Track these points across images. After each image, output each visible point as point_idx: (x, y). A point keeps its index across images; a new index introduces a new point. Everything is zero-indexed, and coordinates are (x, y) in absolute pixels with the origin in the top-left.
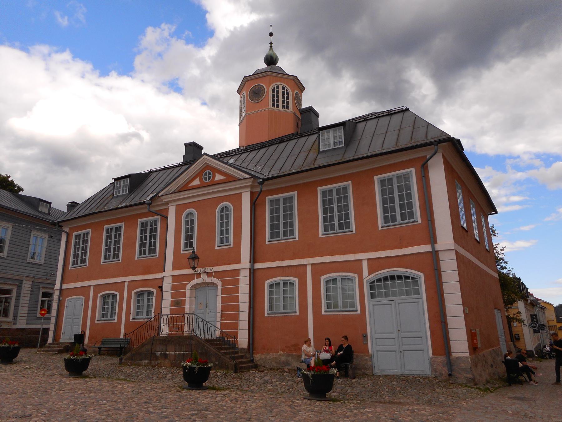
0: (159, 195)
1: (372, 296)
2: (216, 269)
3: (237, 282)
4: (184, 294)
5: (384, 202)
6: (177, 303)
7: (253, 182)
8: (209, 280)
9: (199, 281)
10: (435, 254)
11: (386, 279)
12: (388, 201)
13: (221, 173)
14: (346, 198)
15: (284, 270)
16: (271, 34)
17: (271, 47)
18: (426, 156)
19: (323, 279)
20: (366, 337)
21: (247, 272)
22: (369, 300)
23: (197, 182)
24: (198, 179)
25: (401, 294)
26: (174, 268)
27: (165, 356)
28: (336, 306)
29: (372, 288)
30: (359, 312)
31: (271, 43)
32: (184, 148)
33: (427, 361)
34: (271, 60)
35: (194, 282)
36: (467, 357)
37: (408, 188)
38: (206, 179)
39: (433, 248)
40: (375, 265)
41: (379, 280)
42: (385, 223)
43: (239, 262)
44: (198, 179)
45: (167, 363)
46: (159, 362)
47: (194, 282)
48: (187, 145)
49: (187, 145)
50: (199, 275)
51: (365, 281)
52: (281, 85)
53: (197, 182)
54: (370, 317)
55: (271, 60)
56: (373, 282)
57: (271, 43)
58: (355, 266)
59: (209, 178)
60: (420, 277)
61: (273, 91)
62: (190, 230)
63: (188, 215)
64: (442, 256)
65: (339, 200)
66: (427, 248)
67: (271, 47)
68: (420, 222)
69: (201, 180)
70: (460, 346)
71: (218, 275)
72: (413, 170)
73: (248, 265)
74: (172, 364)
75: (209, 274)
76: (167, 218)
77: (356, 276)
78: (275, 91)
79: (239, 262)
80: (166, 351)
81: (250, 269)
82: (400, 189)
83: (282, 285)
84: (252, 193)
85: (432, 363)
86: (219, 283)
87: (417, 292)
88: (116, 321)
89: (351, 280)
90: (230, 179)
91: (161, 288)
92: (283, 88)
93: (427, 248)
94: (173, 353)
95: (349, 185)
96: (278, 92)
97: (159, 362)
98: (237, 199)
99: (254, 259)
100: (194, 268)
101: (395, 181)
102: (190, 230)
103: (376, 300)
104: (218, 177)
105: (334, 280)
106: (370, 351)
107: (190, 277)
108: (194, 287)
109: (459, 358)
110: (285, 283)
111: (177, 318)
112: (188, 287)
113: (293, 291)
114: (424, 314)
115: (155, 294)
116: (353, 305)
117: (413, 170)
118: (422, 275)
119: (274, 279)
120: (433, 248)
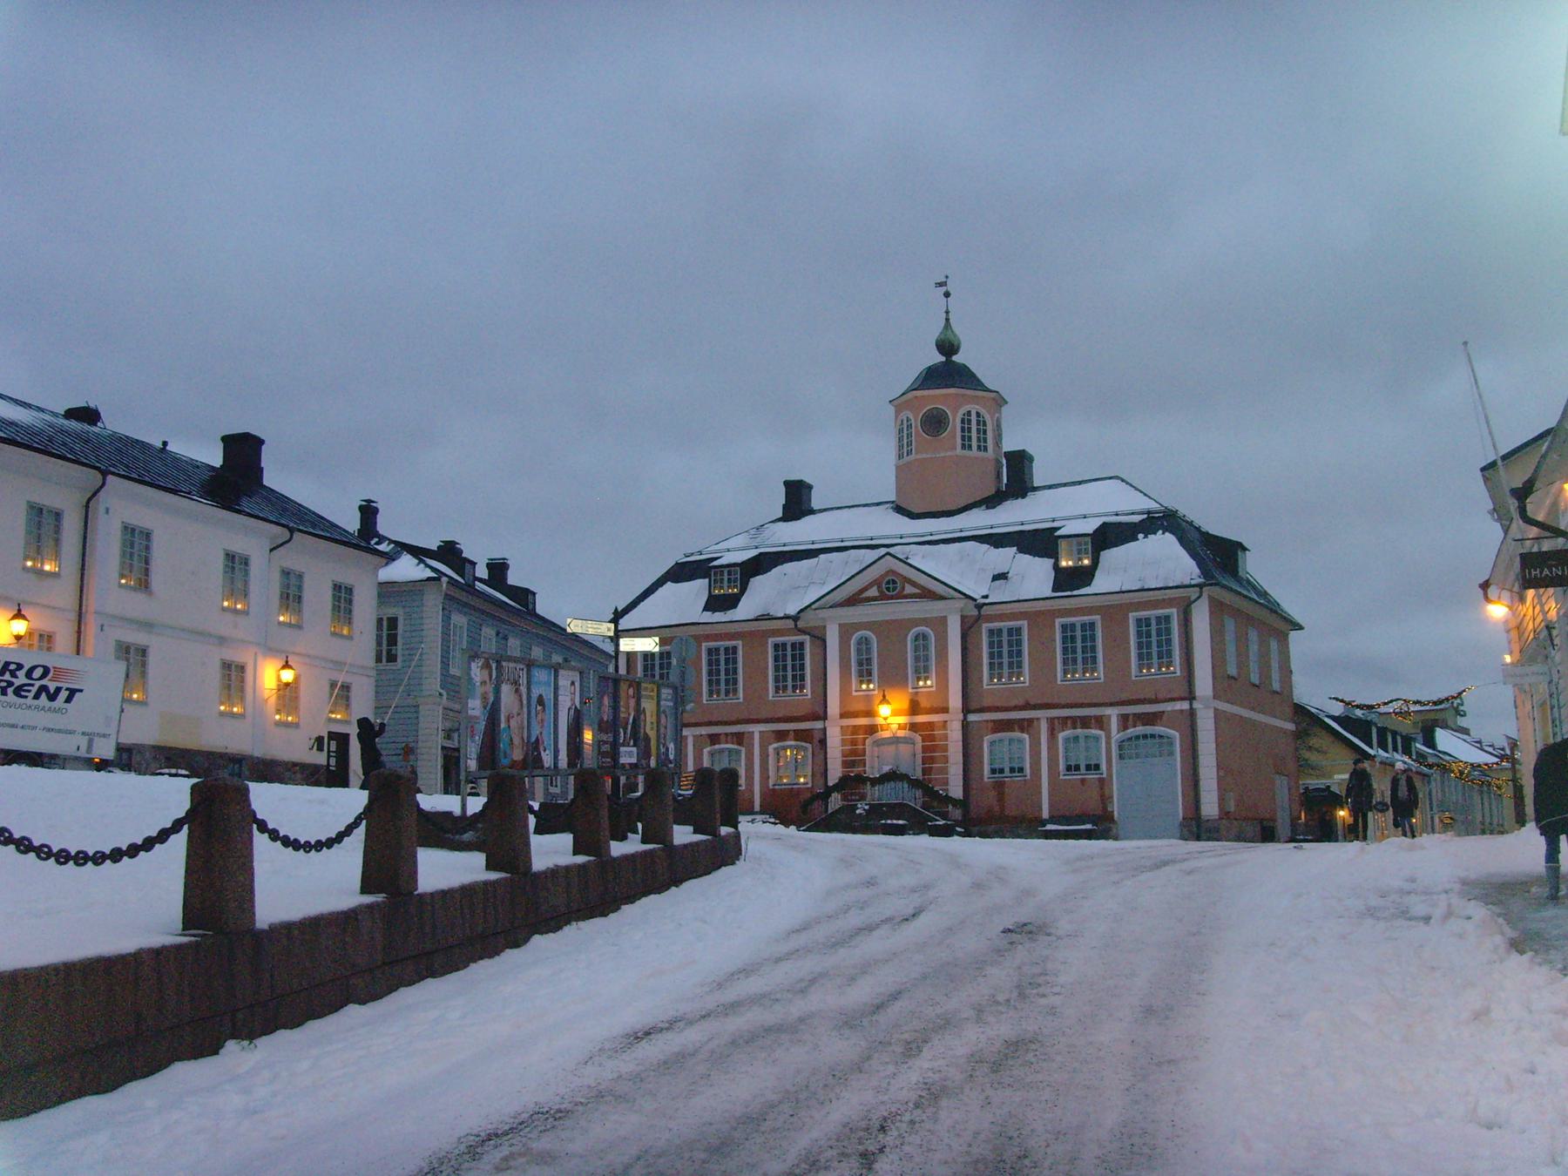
1: (1121, 757)
10: (1192, 713)
13: (914, 584)
16: (947, 295)
17: (947, 320)
19: (1061, 736)
29: (1120, 748)
31: (947, 312)
34: (947, 347)
37: (1168, 631)
48: (787, 484)
49: (787, 484)
52: (974, 408)
53: (873, 592)
55: (947, 347)
57: (947, 312)
61: (963, 421)
63: (859, 643)
65: (1084, 639)
67: (947, 320)
76: (824, 641)
78: (966, 421)
84: (963, 618)
87: (1171, 754)
89: (1097, 739)
92: (978, 414)
96: (969, 421)
104: (909, 589)
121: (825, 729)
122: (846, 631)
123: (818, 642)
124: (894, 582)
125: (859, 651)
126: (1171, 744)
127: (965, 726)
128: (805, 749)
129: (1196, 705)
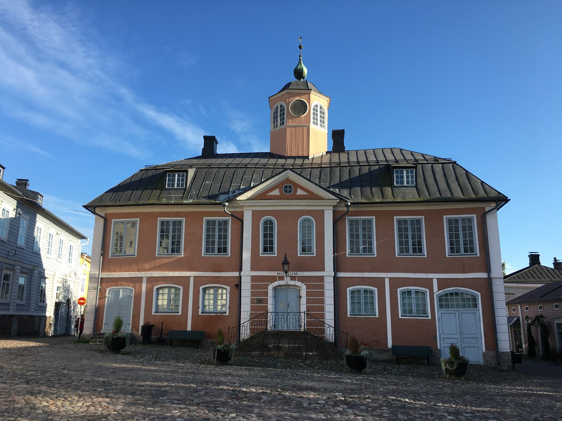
0: (238, 198)
1: (441, 306)
2: (300, 274)
3: (322, 287)
4: (266, 294)
5: (451, 237)
6: (259, 301)
7: (338, 203)
8: (293, 283)
9: (282, 283)
11: (451, 294)
12: (454, 236)
14: (419, 230)
15: (364, 281)
18: (484, 208)
20: (435, 336)
21: (332, 280)
22: (438, 310)
23: (276, 192)
24: (278, 190)
25: (458, 306)
26: (252, 269)
27: (279, 348)
28: (411, 311)
29: (440, 300)
30: (430, 318)
32: (202, 140)
33: (481, 354)
35: (276, 284)
36: (508, 352)
37: (471, 228)
38: (286, 191)
39: (489, 275)
40: (442, 283)
41: (446, 295)
42: (451, 252)
43: (323, 269)
44: (278, 190)
45: (281, 354)
46: (272, 353)
47: (276, 284)
49: (205, 137)
50: (281, 278)
51: (435, 295)
53: (276, 192)
54: (439, 322)
56: (442, 296)
58: (428, 283)
59: (290, 191)
60: (478, 295)
62: (268, 236)
63: (266, 222)
64: (494, 282)
66: (484, 275)
68: (478, 255)
69: (280, 191)
70: (505, 344)
71: (302, 279)
72: (475, 216)
73: (333, 274)
74: (286, 354)
75: (293, 278)
76: (242, 221)
77: (428, 290)
79: (323, 269)
80: (279, 343)
81: (334, 277)
82: (464, 228)
83: (362, 292)
84: (334, 212)
85: (484, 355)
86: (303, 287)
87: (475, 306)
88: (180, 314)
89: (423, 293)
90: (312, 196)
91: (238, 286)
93: (484, 275)
94: (287, 346)
95: (422, 218)
97: (272, 353)
98: (319, 216)
99: (336, 269)
100: (286, 272)
101: (460, 222)
102: (268, 236)
103: (443, 310)
104: (300, 192)
105: (409, 292)
106: (439, 347)
107: (273, 279)
108: (275, 289)
109: (503, 353)
110: (366, 291)
111: (259, 314)
112: (270, 287)
113: (372, 298)
114: (480, 321)
115: (229, 291)
116: (425, 312)
117: (475, 216)
118: (479, 294)
119: (355, 287)
120: (489, 275)
121: (240, 277)
122: (256, 216)
123: (240, 222)
124: (290, 187)
125: (265, 229)
126: (475, 299)
127: (336, 279)
128: (226, 289)
129: (493, 275)
